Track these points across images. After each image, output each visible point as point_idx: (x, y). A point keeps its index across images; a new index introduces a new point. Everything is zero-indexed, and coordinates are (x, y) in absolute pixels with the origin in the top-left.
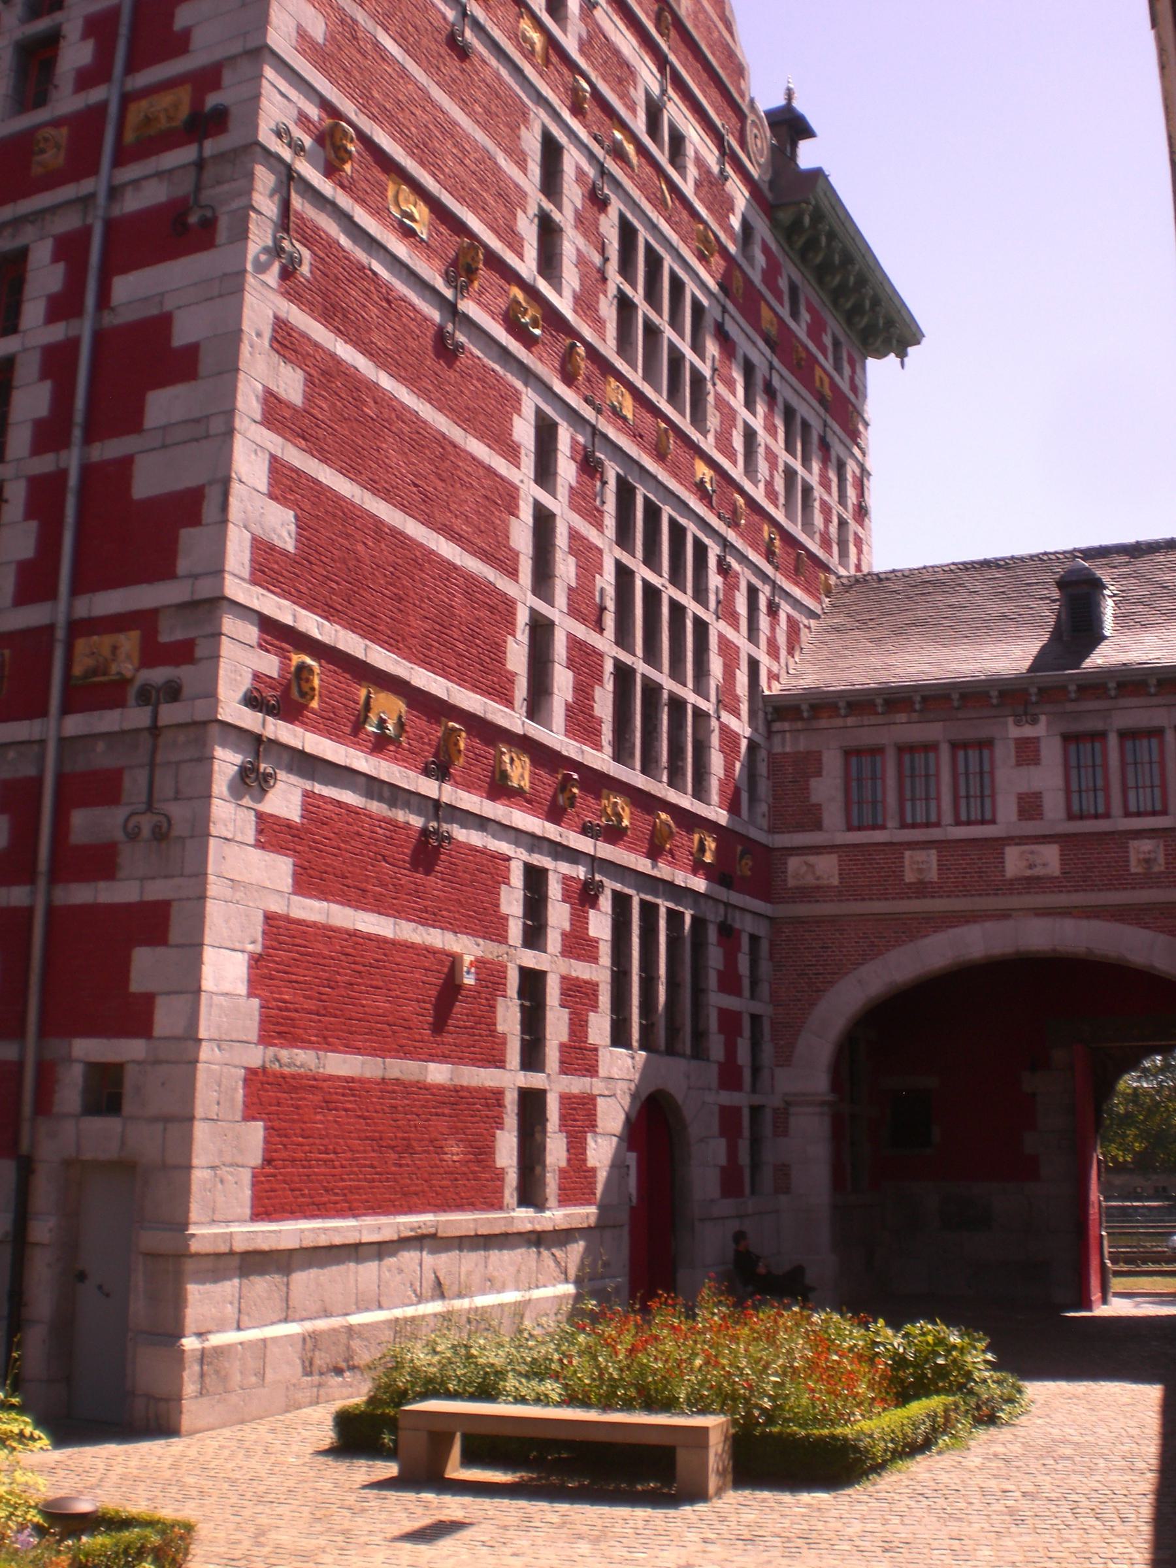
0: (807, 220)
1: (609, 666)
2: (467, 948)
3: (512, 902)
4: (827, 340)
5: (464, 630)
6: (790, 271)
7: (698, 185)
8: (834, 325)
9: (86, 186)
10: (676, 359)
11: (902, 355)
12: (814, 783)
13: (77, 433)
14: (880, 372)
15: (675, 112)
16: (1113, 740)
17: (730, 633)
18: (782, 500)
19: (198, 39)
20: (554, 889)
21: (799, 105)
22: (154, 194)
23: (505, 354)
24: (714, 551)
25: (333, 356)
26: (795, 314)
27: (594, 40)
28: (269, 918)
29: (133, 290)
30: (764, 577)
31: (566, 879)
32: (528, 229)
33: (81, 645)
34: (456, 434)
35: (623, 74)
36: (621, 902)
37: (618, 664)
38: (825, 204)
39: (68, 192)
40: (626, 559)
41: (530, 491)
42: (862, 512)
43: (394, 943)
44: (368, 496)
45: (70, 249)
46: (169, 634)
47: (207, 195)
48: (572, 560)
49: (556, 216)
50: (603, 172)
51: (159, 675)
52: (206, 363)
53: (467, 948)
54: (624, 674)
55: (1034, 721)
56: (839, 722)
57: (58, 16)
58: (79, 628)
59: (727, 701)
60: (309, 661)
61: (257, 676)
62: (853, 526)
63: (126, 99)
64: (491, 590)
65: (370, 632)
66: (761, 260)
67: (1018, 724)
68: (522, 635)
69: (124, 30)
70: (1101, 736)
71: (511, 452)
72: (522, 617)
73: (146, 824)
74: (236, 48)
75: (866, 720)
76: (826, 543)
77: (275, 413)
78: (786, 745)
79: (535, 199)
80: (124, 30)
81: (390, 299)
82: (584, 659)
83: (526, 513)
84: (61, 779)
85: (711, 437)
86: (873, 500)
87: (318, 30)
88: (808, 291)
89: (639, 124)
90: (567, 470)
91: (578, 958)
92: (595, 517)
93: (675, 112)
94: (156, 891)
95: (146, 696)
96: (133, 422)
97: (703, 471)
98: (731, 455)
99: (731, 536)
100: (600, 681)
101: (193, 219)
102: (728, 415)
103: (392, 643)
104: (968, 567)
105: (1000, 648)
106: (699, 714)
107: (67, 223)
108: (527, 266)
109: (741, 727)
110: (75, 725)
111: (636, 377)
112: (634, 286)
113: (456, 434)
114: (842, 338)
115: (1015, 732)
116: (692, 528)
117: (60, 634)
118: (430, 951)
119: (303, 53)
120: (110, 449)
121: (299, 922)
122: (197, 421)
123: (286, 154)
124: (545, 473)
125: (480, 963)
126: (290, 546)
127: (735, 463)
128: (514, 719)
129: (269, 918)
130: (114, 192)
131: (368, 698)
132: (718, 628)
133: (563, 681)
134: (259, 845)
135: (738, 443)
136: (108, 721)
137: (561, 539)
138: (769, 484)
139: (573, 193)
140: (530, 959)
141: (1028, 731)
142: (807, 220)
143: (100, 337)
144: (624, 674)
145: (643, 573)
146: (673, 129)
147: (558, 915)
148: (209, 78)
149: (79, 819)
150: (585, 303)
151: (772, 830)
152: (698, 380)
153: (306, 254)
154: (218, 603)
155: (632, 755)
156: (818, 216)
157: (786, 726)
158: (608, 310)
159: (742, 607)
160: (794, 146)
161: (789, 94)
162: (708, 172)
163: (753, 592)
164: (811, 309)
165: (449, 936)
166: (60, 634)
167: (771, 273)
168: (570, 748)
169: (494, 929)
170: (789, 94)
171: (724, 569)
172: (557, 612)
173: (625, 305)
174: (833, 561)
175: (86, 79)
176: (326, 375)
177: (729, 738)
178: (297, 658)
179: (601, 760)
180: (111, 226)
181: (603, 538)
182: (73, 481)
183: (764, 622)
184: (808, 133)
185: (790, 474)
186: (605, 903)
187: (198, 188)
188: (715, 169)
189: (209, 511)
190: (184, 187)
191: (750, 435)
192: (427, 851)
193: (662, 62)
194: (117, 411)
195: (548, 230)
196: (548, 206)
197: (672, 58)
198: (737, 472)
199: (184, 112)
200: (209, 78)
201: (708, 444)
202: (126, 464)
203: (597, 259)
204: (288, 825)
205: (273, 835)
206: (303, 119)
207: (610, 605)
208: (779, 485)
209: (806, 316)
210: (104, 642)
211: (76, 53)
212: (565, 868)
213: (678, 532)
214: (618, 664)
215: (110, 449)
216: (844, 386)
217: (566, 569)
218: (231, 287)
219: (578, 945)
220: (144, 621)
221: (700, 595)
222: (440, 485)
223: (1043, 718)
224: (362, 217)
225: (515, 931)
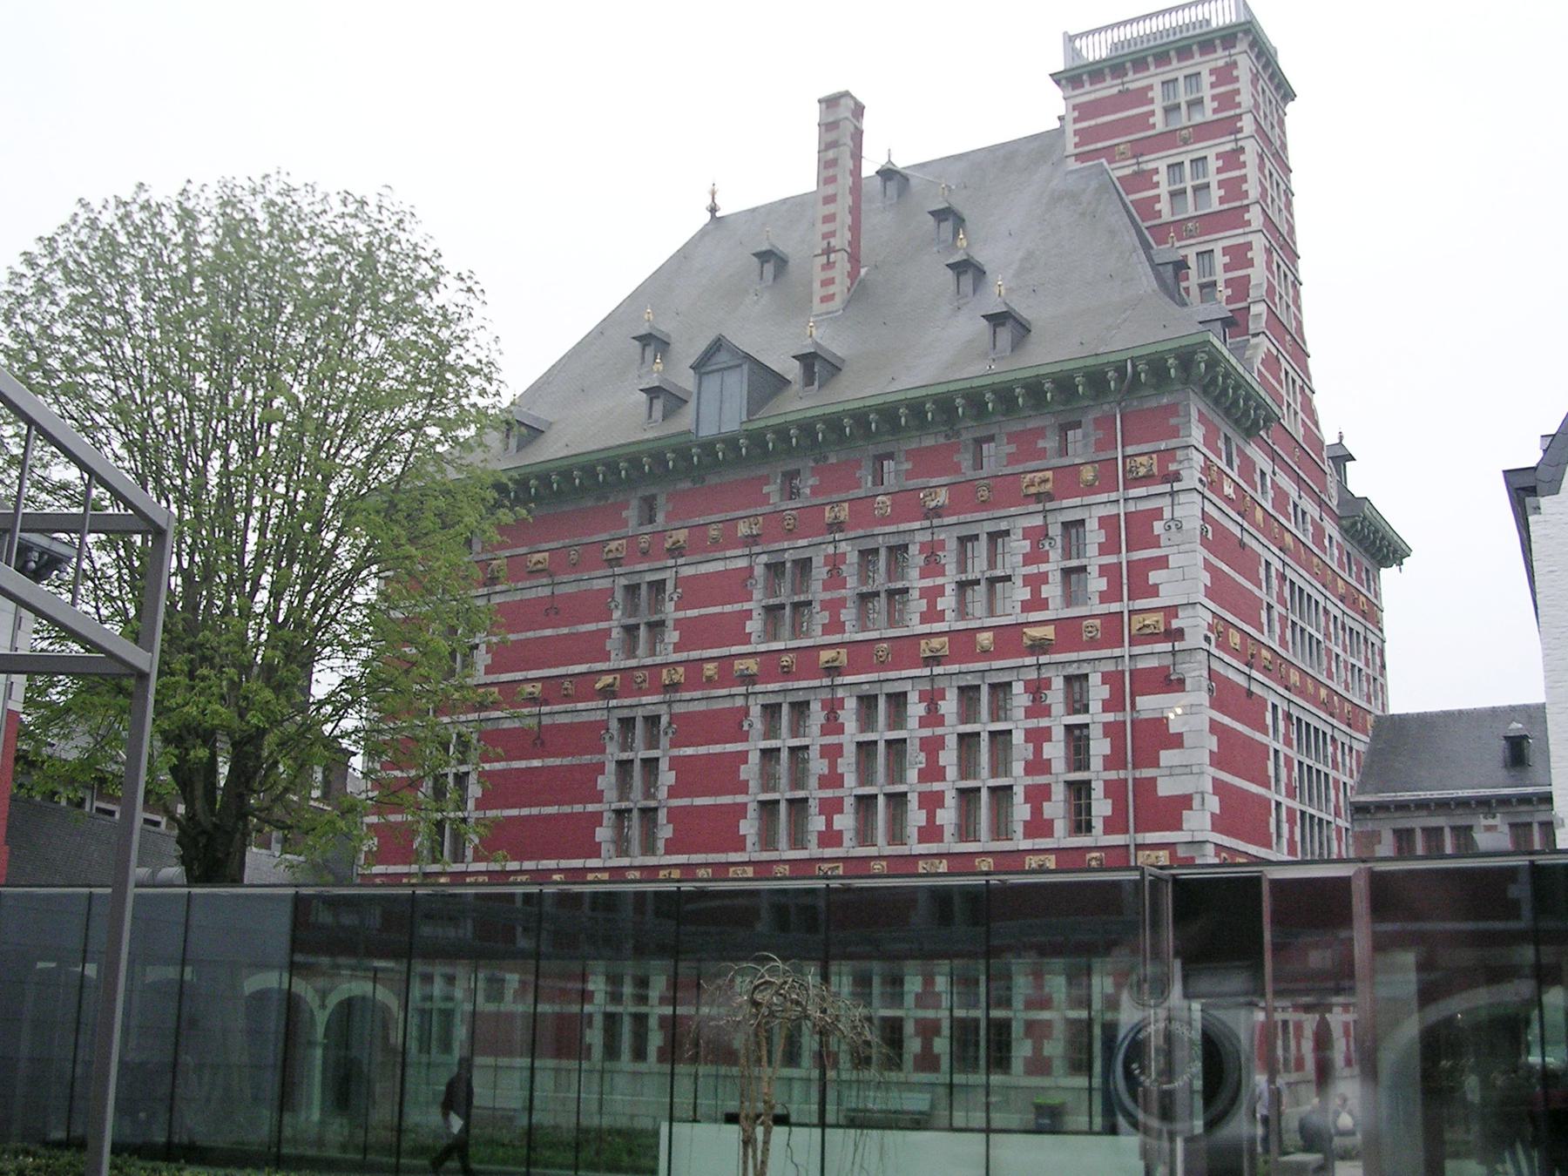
9: (1117, 652)
16: (1536, 828)
22: (1153, 663)
29: (1148, 704)
46: (1182, 852)
52: (1187, 742)
58: (1139, 847)
70: (1530, 825)
96: (1155, 763)
107: (1110, 667)
115: (1484, 822)
120: (1147, 773)
141: (1491, 822)
161: (1341, 438)
170: (1341, 438)
189: (1196, 803)
190: (1168, 661)
200: (1171, 611)
202: (1154, 780)
215: (1147, 773)
216: (1371, 597)
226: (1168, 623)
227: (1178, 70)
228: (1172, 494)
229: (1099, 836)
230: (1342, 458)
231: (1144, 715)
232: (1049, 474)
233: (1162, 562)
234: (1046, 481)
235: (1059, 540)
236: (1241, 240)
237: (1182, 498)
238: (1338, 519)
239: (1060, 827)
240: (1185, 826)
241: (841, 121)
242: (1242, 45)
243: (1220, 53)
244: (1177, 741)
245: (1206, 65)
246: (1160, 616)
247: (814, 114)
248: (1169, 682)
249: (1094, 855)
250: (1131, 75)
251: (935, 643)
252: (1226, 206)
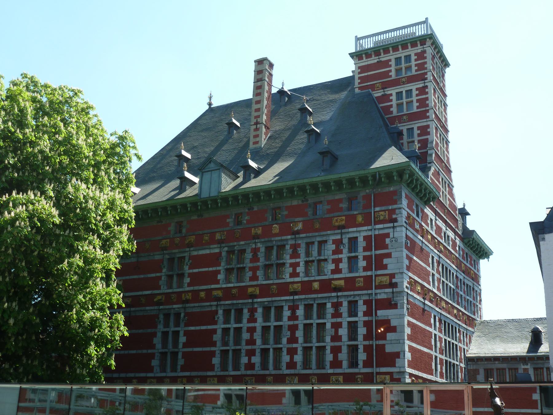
9: (370, 292)
11: (488, 258)
12: (478, 376)
14: (483, 263)
19: (389, 267)
29: (382, 314)
33: (378, 376)
45: (368, 303)
46: (396, 376)
52: (398, 330)
55: (527, 365)
56: (483, 363)
58: (378, 373)
59: (461, 362)
67: (523, 365)
70: (543, 368)
78: (471, 367)
104: (509, 321)
105: (518, 345)
107: (366, 298)
109: (463, 365)
115: (523, 367)
120: (381, 342)
130: (376, 294)
141: (526, 367)
154: (404, 372)
157: (471, 363)
161: (464, 205)
166: (375, 375)
170: (464, 205)
177: (461, 368)
188: (453, 237)
189: (401, 356)
190: (390, 296)
200: (392, 276)
202: (384, 345)
210: (383, 376)
215: (381, 342)
216: (476, 271)
218: (402, 316)
220: (391, 374)
223: (529, 364)
226: (391, 280)
227: (402, 53)
228: (394, 227)
230: (464, 213)
231: (380, 318)
232: (344, 218)
233: (389, 255)
234: (342, 220)
235: (347, 245)
236: (425, 124)
237: (398, 229)
238: (462, 239)
239: (345, 364)
240: (397, 365)
241: (263, 68)
242: (429, 42)
243: (419, 47)
244: (393, 329)
245: (412, 52)
246: (388, 277)
247: (252, 67)
248: (390, 304)
249: (360, 376)
251: (295, 286)
252: (419, 110)
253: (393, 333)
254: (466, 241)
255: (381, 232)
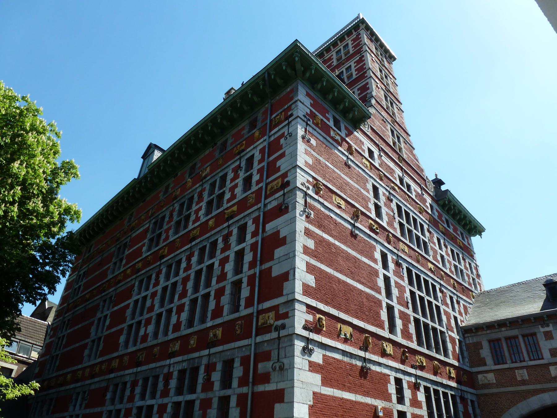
0: (447, 202)
1: (412, 319)
2: (380, 404)
3: (392, 389)
4: (459, 233)
5: (369, 309)
6: (445, 216)
7: (416, 196)
8: (460, 229)
9: (259, 205)
10: (418, 238)
11: (480, 235)
12: (481, 351)
13: (258, 263)
14: (475, 240)
15: (407, 179)
17: (447, 309)
18: (455, 273)
19: (281, 168)
20: (405, 385)
21: (439, 177)
22: (274, 204)
23: (370, 236)
24: (438, 287)
25: (322, 237)
26: (449, 226)
27: (382, 164)
28: (314, 393)
29: (270, 227)
30: (454, 294)
31: (408, 382)
32: (372, 207)
33: (261, 317)
34: (359, 256)
35: (392, 172)
36: (427, 389)
37: (414, 318)
38: (451, 198)
39: (255, 207)
40: (412, 289)
41: (382, 271)
42: (478, 276)
43: (356, 402)
44: (335, 272)
45: (256, 221)
46: (282, 311)
47: (286, 202)
48: (397, 289)
49: (379, 203)
50: (390, 193)
51: (279, 323)
52: (288, 240)
53: (380, 404)
54: (417, 321)
55: (548, 326)
56: (485, 332)
57: (252, 171)
58: (259, 312)
60: (321, 316)
61: (306, 321)
62: (477, 280)
63: (267, 185)
64: (374, 297)
65: (339, 309)
66: (437, 214)
67: (542, 327)
68: (385, 310)
69: (265, 170)
71: (375, 261)
72: (384, 305)
73: (277, 365)
74: (291, 167)
75: (493, 331)
76: (470, 284)
77: (306, 250)
78: (470, 341)
79: (373, 200)
80: (265, 170)
81: (336, 223)
82: (404, 317)
83: (381, 277)
84: (255, 355)
85: (431, 257)
86: (480, 273)
87: (310, 161)
88: (451, 221)
89: (398, 182)
90: (391, 266)
91: (416, 407)
92: (402, 278)
93: (407, 179)
94: (281, 386)
95: (277, 329)
96: (272, 258)
97: (430, 266)
98: (438, 262)
99: (442, 282)
100: (410, 322)
101: (283, 208)
102: (435, 252)
103: (346, 312)
104: (514, 285)
105: (530, 306)
106: (442, 332)
107: (255, 215)
108: (373, 215)
109: (455, 335)
110: (259, 339)
111: (408, 242)
112: (403, 220)
113: (359, 256)
114: (463, 232)
115: (542, 330)
116: (430, 281)
117: (255, 314)
118: (367, 405)
119: (307, 167)
120: (266, 266)
121: (324, 395)
122: (287, 255)
123: (305, 189)
124: (385, 266)
125: (384, 409)
126: (314, 286)
127: (439, 264)
128: (385, 333)
129: (314, 393)
130: (265, 205)
131: (340, 328)
132: (442, 308)
133: (399, 323)
134: (310, 371)
135: (439, 258)
136: (267, 337)
137: (393, 284)
138: (450, 269)
139: (383, 199)
140: (400, 408)
141: (547, 329)
142: (447, 202)
143: (263, 239)
144: (417, 321)
145: (418, 293)
146: (407, 183)
147: (408, 393)
148: (285, 175)
149: (260, 365)
150: (390, 224)
151: (471, 367)
152: (425, 243)
153: (312, 213)
154: (294, 300)
155: (423, 344)
156: (450, 201)
157: (469, 335)
158: (397, 226)
159: (449, 301)
160: (440, 187)
161: (436, 175)
162: (418, 193)
163: (451, 298)
164: (452, 225)
165: (373, 400)
166: (255, 314)
167: (440, 216)
168: (404, 342)
169: (387, 397)
170: (436, 175)
171: (441, 291)
172: (394, 303)
173: (401, 225)
174: (473, 289)
175: (258, 183)
176: (320, 241)
177: (452, 340)
178: (318, 316)
179: (414, 345)
180: (264, 213)
181: (405, 283)
182: (258, 275)
183: (456, 306)
184: (443, 183)
185: (456, 267)
186: (422, 389)
187: (284, 200)
188: (420, 192)
189: (291, 277)
190: (281, 200)
191: (442, 257)
192: (364, 372)
193: (402, 169)
194: (267, 256)
195: (378, 208)
196: (376, 201)
197: (404, 167)
198: (440, 266)
199: (280, 184)
200: (285, 175)
201: (431, 258)
202: (271, 268)
203: (392, 214)
204: (319, 365)
205: (313, 367)
206: (308, 181)
207: (410, 301)
208: (453, 269)
209: (452, 227)
211: (256, 178)
212: (407, 378)
213: (426, 282)
214: (414, 318)
215: (266, 266)
216: (466, 244)
217: (395, 292)
218: (293, 220)
219: (415, 403)
220: (275, 308)
221: (436, 298)
222: (356, 270)
223: (551, 325)
224: (326, 203)
225: (394, 398)
226: (283, 181)
228: (289, 124)
229: (244, 312)
233: (283, 155)
240: (284, 293)
242: (362, 26)
243: (354, 33)
245: (349, 41)
246: (280, 180)
250: (326, 55)
251: (195, 232)
253: (282, 248)
254: (441, 203)
255: (276, 136)
